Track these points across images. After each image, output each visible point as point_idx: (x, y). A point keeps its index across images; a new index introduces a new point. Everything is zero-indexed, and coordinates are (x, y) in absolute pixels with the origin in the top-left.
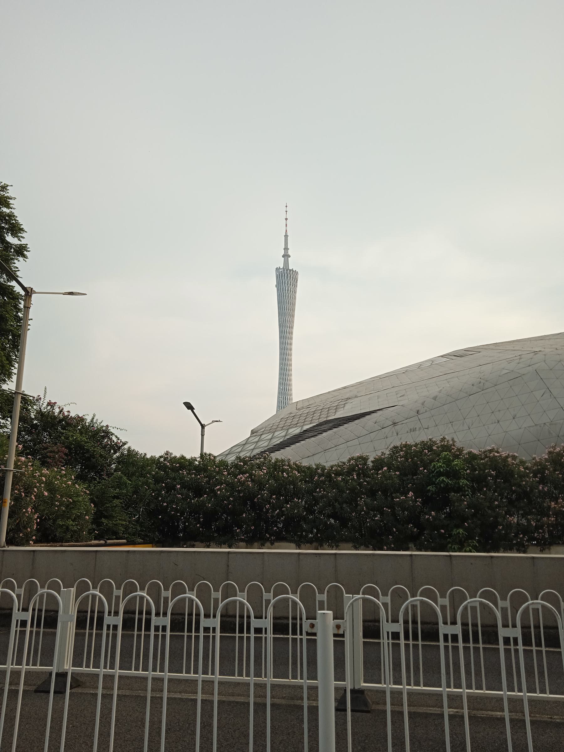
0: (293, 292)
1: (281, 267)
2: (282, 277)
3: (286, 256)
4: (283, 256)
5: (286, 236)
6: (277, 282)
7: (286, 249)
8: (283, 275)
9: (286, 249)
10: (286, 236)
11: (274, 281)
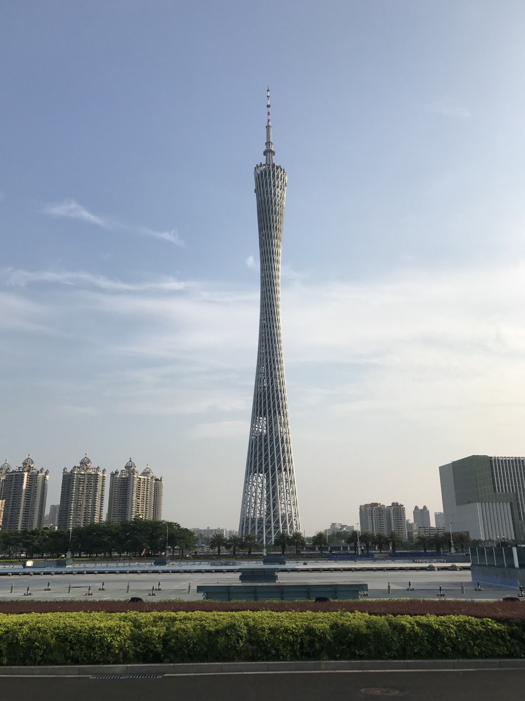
0: (281, 198)
1: (264, 163)
2: (265, 176)
3: (268, 152)
4: (265, 153)
5: (268, 127)
6: (257, 187)
7: (268, 143)
8: (268, 173)
9: (268, 143)
10: (268, 127)
11: (252, 185)
